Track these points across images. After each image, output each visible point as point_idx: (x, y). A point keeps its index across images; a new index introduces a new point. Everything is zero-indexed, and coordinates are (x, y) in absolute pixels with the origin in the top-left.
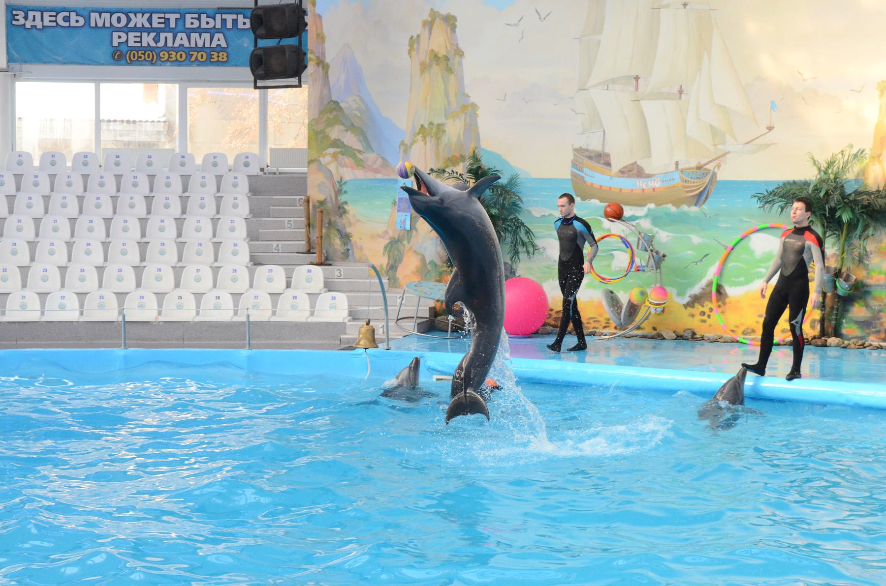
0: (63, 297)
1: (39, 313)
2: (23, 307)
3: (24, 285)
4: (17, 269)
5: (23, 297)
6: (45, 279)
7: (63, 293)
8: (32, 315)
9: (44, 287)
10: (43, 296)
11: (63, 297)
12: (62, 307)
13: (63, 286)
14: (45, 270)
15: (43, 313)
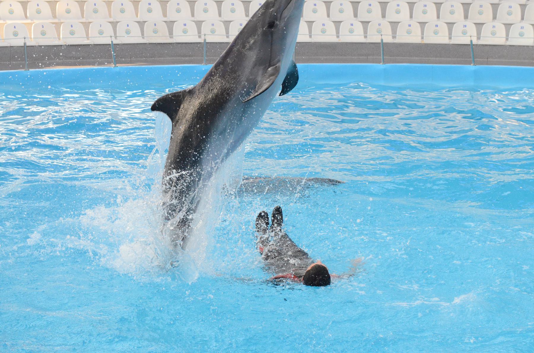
0: (522, 28)
1: (504, 39)
2: (493, 34)
3: (495, 18)
4: (490, 6)
5: (494, 27)
6: (509, 14)
7: (523, 24)
8: (499, 40)
9: (509, 19)
10: (508, 26)
11: (522, 28)
12: (521, 35)
13: (522, 19)
14: (510, 7)
15: (507, 39)
